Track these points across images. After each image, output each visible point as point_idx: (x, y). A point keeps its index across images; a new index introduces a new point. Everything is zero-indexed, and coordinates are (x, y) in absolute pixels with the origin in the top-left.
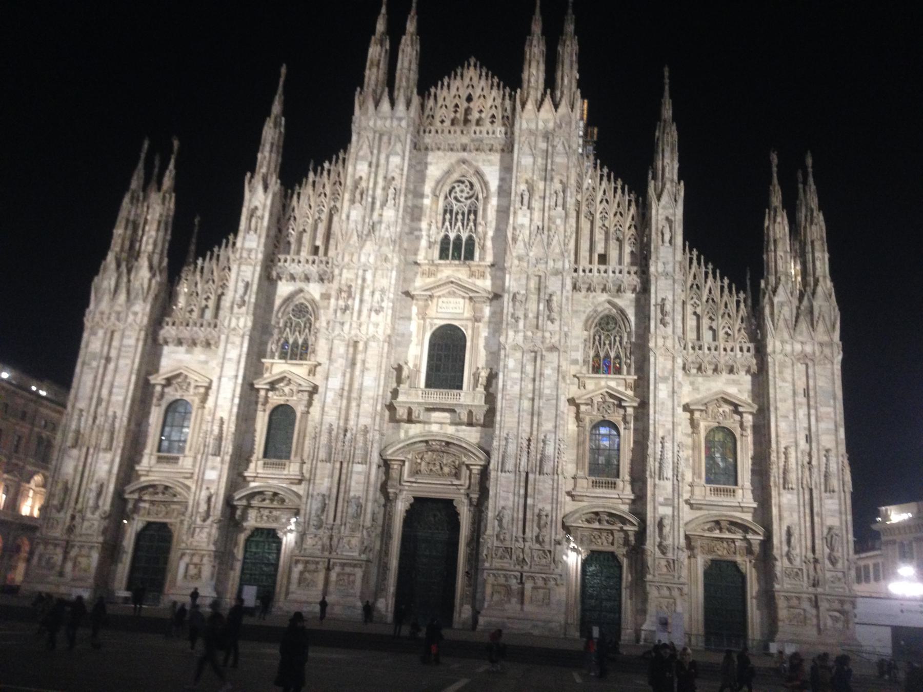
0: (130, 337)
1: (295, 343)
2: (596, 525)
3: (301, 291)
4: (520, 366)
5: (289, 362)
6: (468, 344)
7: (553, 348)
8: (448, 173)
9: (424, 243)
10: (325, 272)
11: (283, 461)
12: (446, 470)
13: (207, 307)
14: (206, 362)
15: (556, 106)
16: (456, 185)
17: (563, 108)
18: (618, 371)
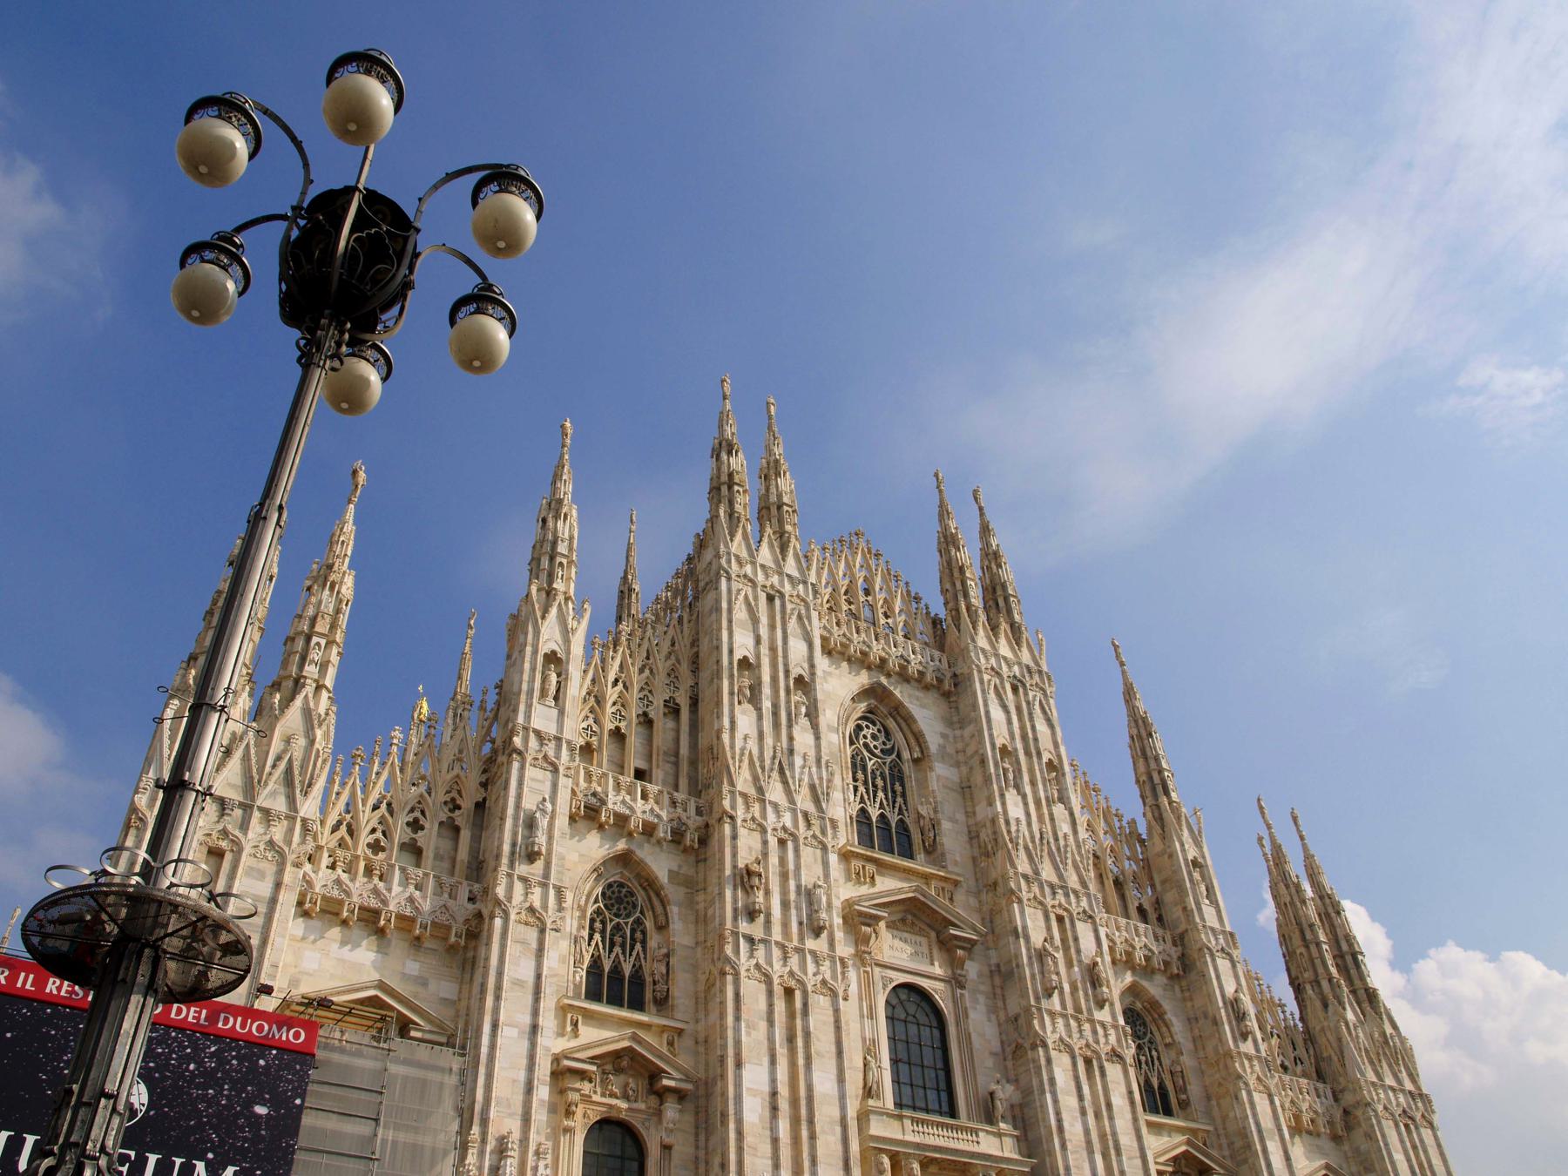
0: (261, 875)
4: (1073, 1084)
5: (625, 1013)
7: (1116, 1056)
16: (864, 724)
17: (1025, 649)
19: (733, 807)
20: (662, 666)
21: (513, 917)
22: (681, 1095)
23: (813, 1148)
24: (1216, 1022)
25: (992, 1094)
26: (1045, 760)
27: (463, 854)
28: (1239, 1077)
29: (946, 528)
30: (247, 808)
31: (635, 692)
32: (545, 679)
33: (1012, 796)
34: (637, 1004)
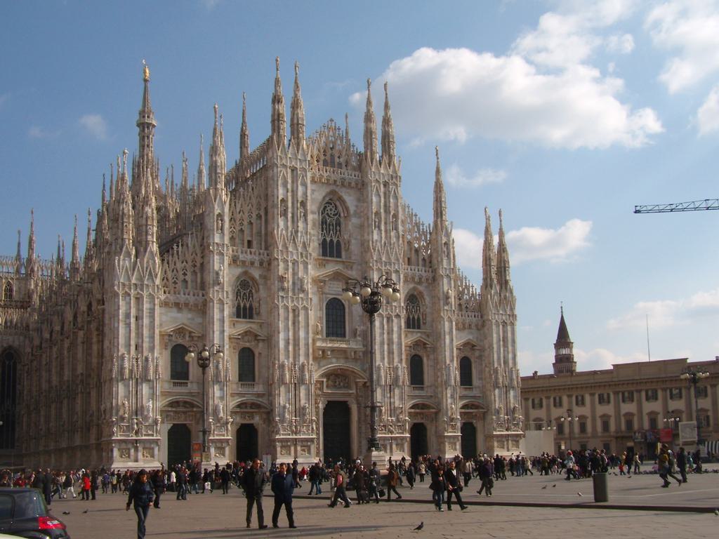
1: (245, 306)
2: (418, 411)
3: (245, 273)
5: (248, 320)
6: (347, 310)
7: (398, 316)
8: (324, 198)
9: (316, 244)
10: (262, 259)
11: (253, 383)
12: (342, 384)
13: (185, 279)
14: (193, 319)
15: (389, 166)
16: (327, 205)
18: (419, 328)
19: (278, 256)
20: (254, 201)
21: (215, 302)
22: (263, 340)
23: (299, 352)
24: (439, 300)
25: (356, 329)
26: (392, 214)
27: (199, 280)
28: (442, 317)
29: (368, 111)
30: (142, 285)
31: (246, 214)
32: (217, 223)
33: (375, 232)
34: (251, 317)
